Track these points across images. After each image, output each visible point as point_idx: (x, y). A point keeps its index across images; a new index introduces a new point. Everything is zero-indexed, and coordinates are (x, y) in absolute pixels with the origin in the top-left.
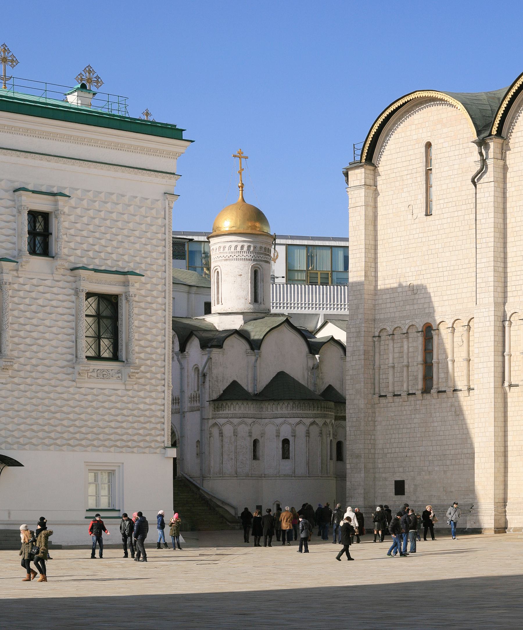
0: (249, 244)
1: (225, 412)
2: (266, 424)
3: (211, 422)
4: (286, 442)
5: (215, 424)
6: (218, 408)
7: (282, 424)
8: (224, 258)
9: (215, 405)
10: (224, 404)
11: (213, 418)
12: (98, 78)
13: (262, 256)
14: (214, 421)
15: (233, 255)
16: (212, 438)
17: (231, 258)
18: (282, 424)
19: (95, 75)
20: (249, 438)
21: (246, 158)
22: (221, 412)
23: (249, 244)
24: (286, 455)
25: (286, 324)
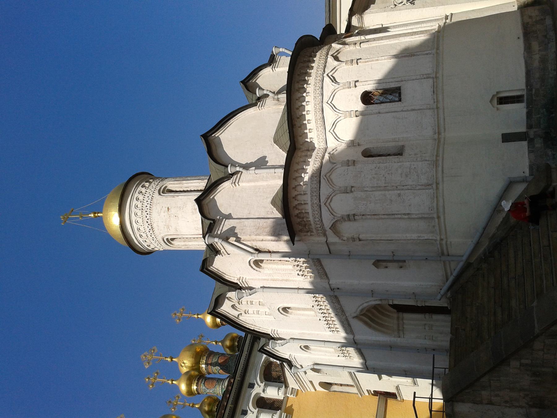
0: (135, 199)
1: (310, 211)
3: (333, 239)
5: (333, 227)
6: (305, 225)
7: (334, 107)
8: (151, 231)
9: (301, 231)
10: (297, 212)
11: (325, 235)
14: (329, 232)
15: (146, 219)
16: (361, 237)
18: (334, 107)
20: (358, 166)
22: (311, 218)
23: (135, 199)
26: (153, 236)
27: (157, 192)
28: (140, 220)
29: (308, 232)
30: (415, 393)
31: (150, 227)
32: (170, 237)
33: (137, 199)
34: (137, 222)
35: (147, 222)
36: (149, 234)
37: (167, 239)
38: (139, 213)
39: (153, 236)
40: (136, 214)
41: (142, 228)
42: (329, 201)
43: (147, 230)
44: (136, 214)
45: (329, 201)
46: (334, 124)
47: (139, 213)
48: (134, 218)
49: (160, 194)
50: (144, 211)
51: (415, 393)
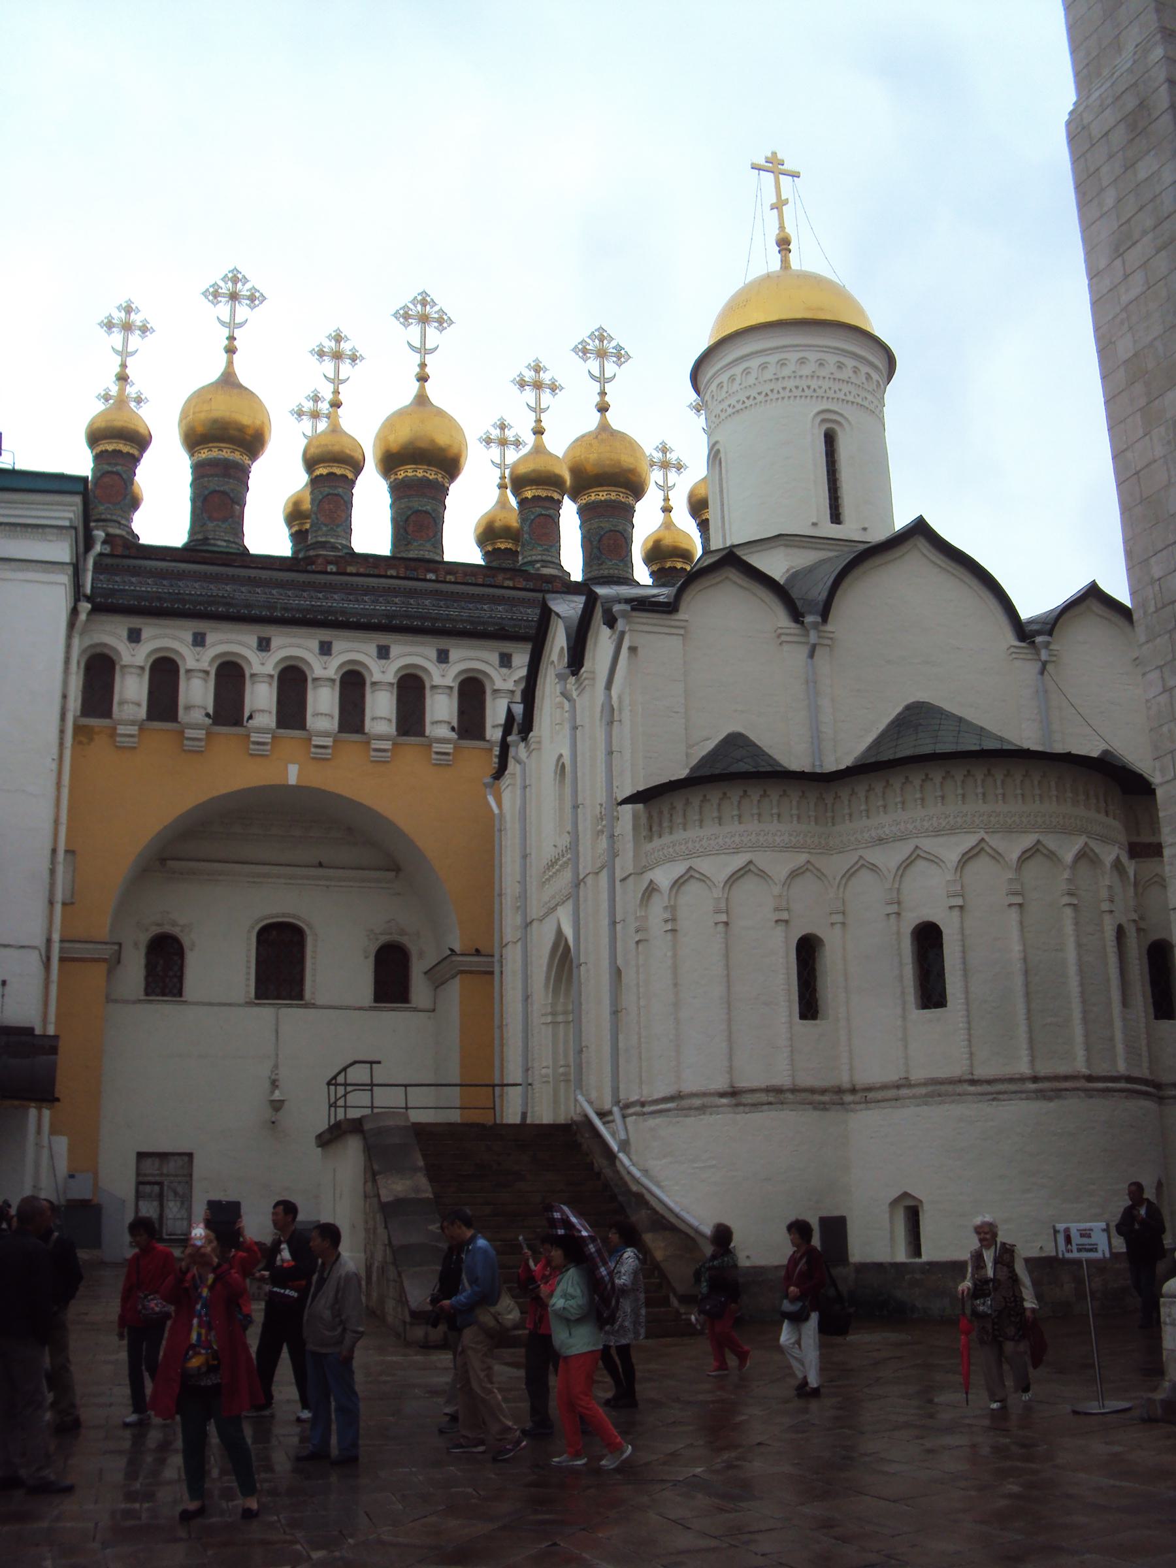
0: (801, 355)
2: (850, 874)
4: (928, 938)
5: (651, 889)
7: (907, 864)
8: (730, 411)
12: (619, 348)
13: (846, 388)
15: (753, 393)
17: (748, 403)
18: (907, 864)
19: (613, 344)
21: (795, 175)
23: (801, 355)
24: (931, 992)
25: (922, 543)
26: (723, 416)
27: (825, 405)
28: (751, 380)
29: (651, 829)
30: (379, 1062)
31: (739, 406)
32: (722, 455)
33: (802, 361)
34: (747, 372)
35: (748, 398)
36: (724, 405)
37: (718, 451)
38: (768, 374)
39: (723, 416)
40: (764, 367)
41: (736, 386)
42: (697, 876)
43: (733, 401)
44: (764, 367)
45: (697, 876)
46: (873, 868)
47: (768, 374)
48: (754, 363)
49: (819, 413)
50: (772, 385)
51: (379, 1062)
